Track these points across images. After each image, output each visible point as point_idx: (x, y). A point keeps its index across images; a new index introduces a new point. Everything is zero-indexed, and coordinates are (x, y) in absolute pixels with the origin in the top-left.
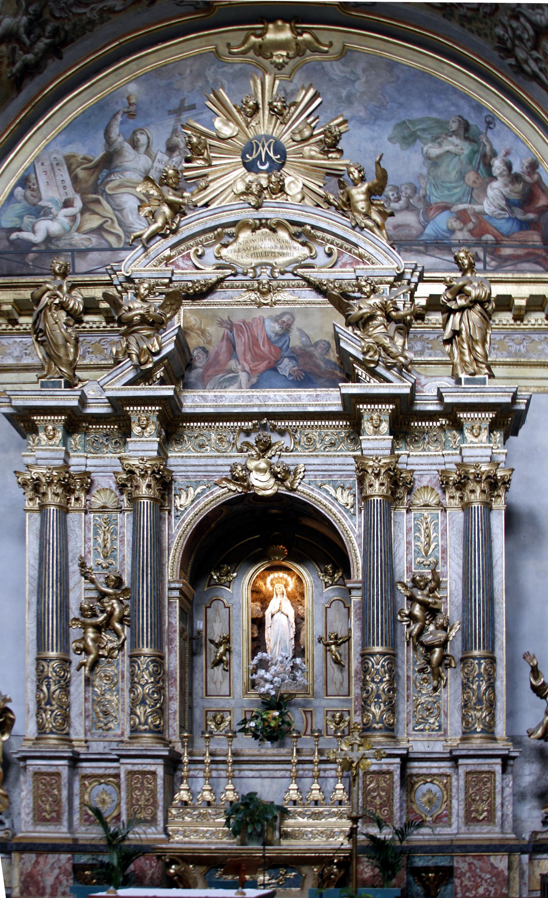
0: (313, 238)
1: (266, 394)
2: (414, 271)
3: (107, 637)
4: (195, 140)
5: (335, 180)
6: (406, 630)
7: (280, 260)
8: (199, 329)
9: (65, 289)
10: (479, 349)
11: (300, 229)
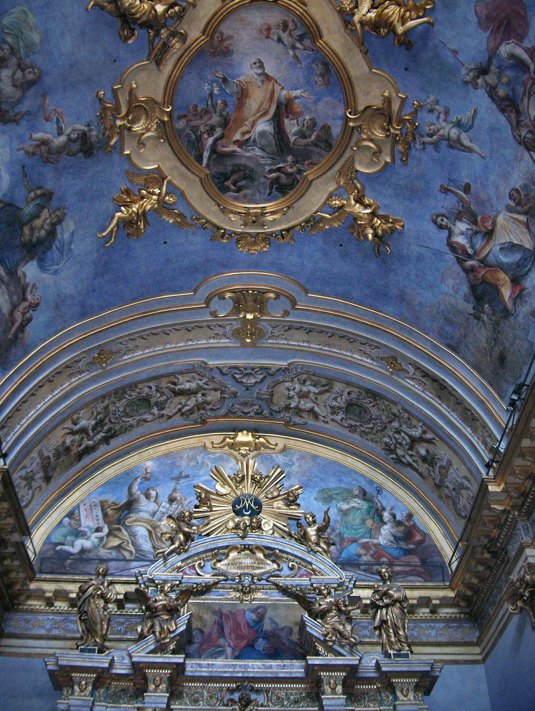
0: (280, 558)
1: (246, 663)
2: (351, 580)
4: (203, 495)
5: (295, 522)
7: (258, 571)
8: (198, 616)
9: (106, 584)
10: (401, 633)
11: (271, 552)
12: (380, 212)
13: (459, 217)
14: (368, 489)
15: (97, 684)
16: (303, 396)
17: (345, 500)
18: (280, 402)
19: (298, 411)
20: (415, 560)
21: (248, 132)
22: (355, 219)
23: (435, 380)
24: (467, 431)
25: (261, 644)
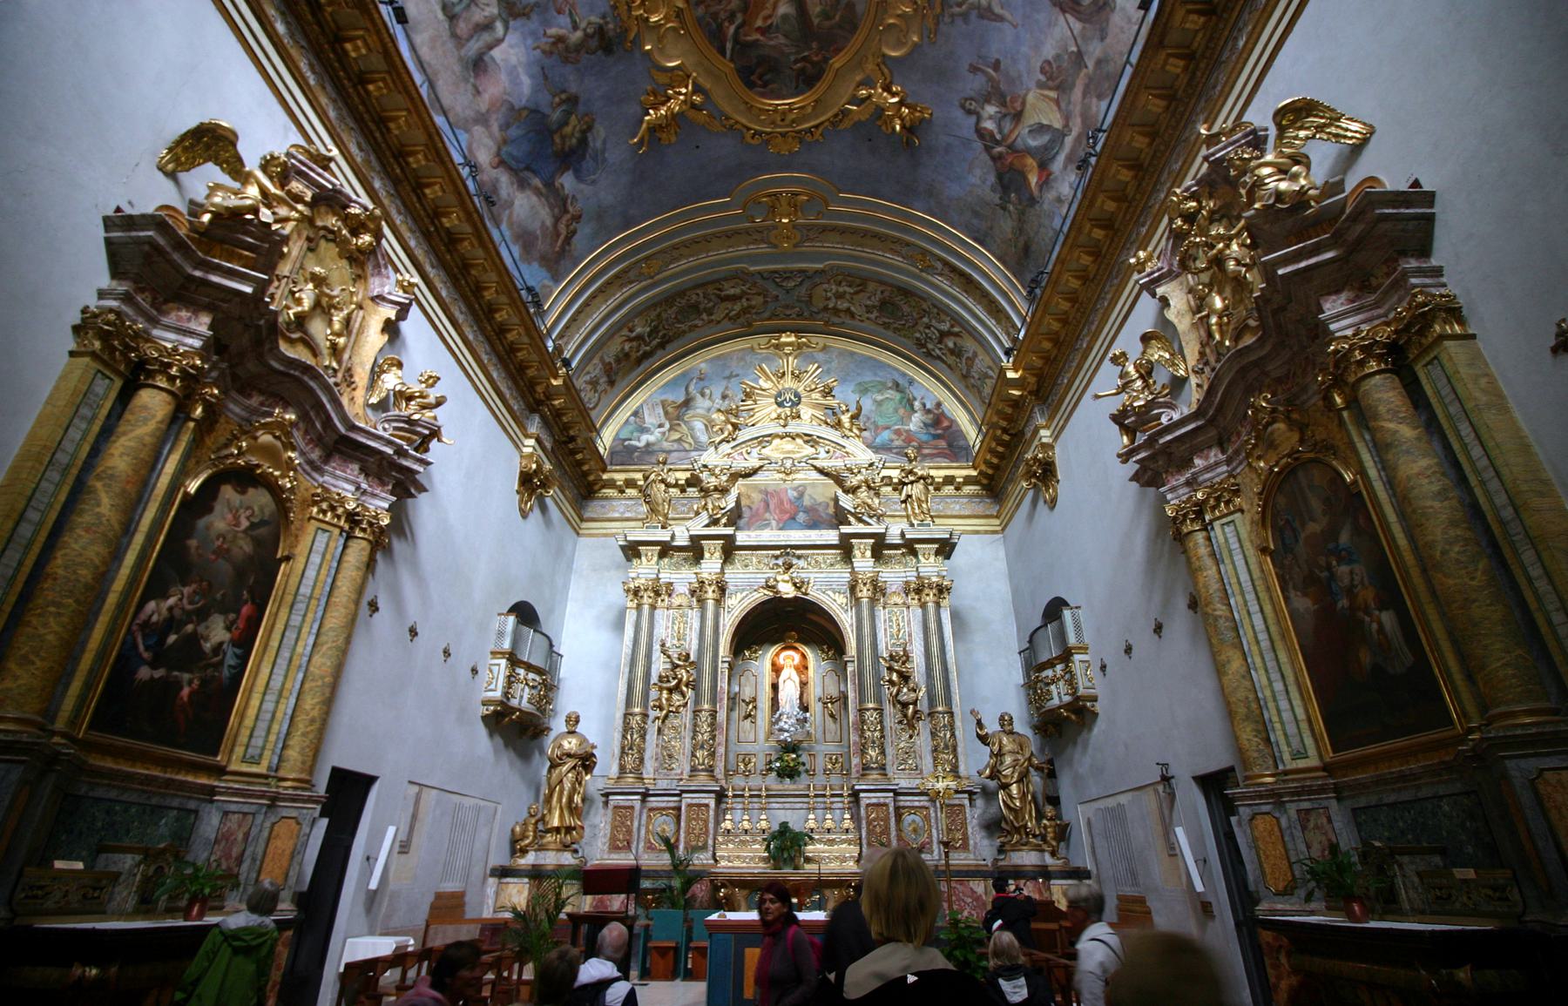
3: (676, 697)
6: (888, 691)
12: (909, 101)
13: (988, 101)
14: (901, 381)
15: (662, 555)
16: (839, 296)
17: (879, 391)
18: (819, 304)
19: (836, 311)
20: (943, 444)
21: (770, 16)
22: (883, 110)
23: (962, 274)
24: (991, 323)
25: (801, 517)
